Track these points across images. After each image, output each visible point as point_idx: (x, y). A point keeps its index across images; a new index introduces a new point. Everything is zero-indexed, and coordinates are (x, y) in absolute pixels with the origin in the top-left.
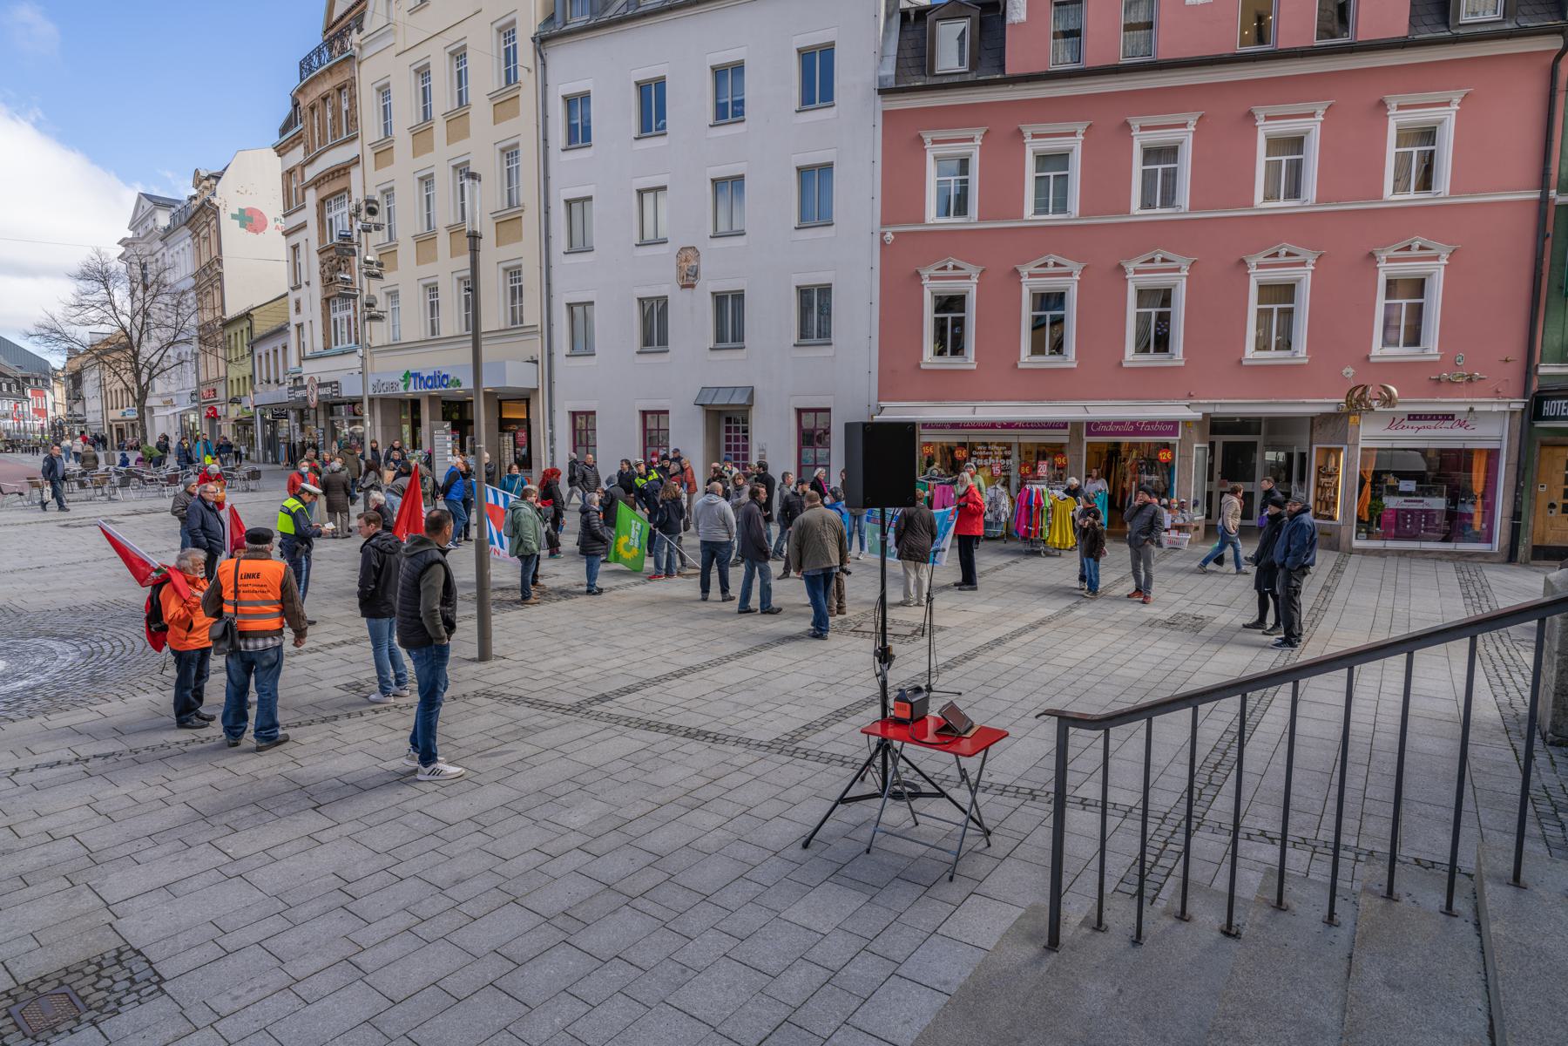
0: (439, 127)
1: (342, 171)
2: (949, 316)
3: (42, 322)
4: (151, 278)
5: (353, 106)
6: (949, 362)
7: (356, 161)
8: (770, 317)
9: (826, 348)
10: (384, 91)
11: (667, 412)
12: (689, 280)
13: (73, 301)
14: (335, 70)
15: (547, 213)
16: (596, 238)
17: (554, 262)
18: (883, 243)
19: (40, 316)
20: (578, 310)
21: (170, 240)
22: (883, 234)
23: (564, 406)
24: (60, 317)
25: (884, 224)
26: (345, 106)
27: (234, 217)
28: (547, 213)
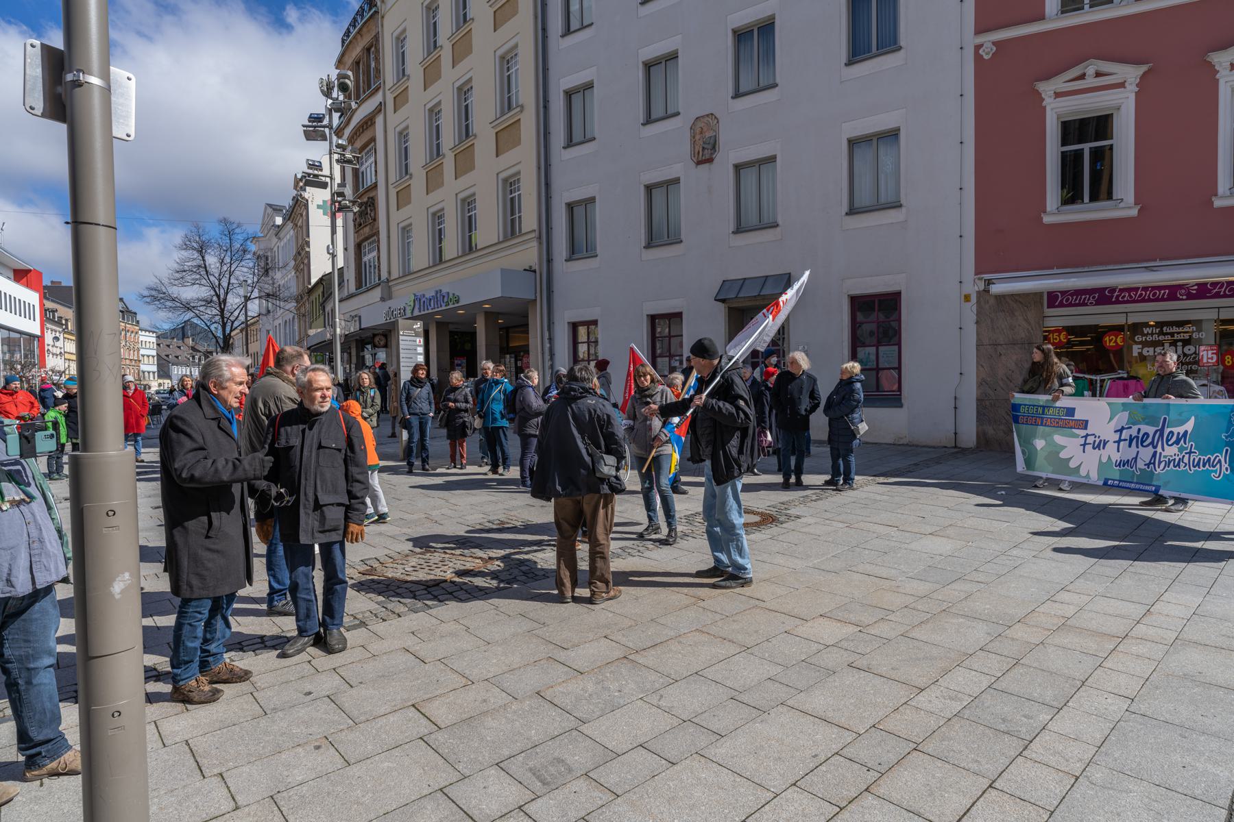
0: (446, 54)
1: (368, 122)
2: (1086, 147)
3: (152, 285)
4: (237, 245)
5: (377, 60)
6: (1087, 212)
7: (380, 108)
8: (810, 182)
9: (892, 212)
10: (400, 40)
11: (679, 315)
12: (705, 153)
13: (176, 266)
14: (365, 29)
15: (545, 107)
16: (597, 128)
17: (554, 161)
18: (978, 58)
19: (151, 281)
20: (579, 211)
21: (281, 235)
22: (978, 47)
23: (564, 316)
24: (166, 281)
25: (978, 31)
26: (373, 65)
27: (319, 207)
28: (545, 107)
